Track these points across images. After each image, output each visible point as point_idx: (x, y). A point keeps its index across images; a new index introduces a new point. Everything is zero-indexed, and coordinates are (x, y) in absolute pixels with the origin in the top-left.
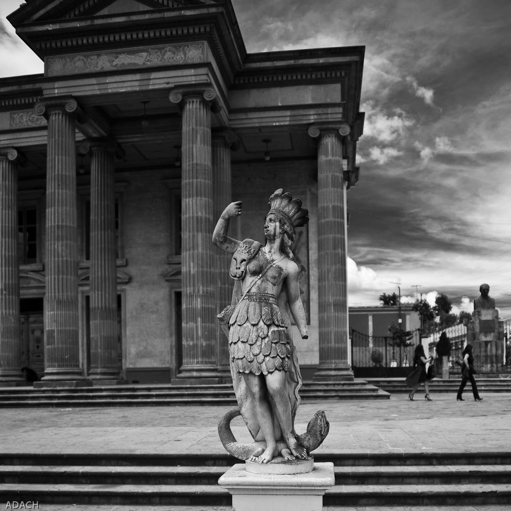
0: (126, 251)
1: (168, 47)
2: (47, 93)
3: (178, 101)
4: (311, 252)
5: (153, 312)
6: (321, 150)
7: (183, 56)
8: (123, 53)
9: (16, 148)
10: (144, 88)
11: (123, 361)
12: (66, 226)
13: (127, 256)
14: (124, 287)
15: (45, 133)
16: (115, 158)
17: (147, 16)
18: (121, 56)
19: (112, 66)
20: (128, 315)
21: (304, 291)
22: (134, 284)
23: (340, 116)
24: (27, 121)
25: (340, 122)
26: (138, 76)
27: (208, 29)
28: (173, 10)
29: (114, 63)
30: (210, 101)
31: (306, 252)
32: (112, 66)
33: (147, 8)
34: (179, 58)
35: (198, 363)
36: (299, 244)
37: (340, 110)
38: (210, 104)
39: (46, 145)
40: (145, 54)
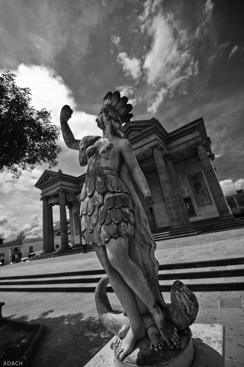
1: (146, 139)
4: (205, 182)
5: (162, 210)
8: (135, 144)
10: (142, 151)
11: (157, 226)
14: (152, 205)
17: (138, 133)
18: (135, 146)
20: (155, 212)
26: (140, 149)
27: (155, 130)
28: (144, 129)
31: (204, 182)
33: (137, 132)
34: (149, 140)
35: (176, 223)
37: (201, 137)
40: (140, 143)
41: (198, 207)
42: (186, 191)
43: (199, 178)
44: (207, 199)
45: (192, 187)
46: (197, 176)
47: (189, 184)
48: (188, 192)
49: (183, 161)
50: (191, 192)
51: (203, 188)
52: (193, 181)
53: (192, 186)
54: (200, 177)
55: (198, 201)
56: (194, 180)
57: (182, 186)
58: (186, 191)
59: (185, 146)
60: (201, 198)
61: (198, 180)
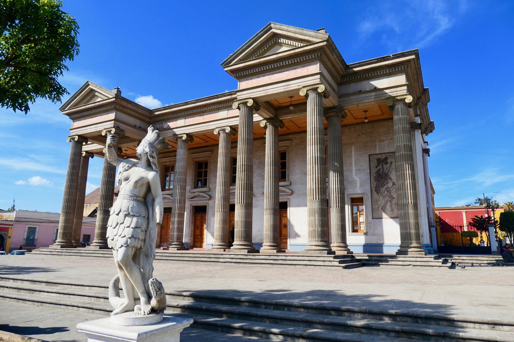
0: (290, 177)
2: (239, 98)
3: (304, 95)
6: (395, 112)
7: (307, 71)
9: (230, 126)
12: (249, 165)
13: (291, 180)
14: (289, 197)
15: (238, 118)
16: (279, 127)
19: (270, 80)
21: (396, 197)
22: (294, 195)
23: (406, 91)
24: (235, 113)
25: (406, 95)
27: (319, 55)
29: (272, 79)
30: (322, 92)
32: (270, 80)
36: (391, 169)
37: (406, 88)
38: (323, 94)
39: (238, 125)
41: (373, 218)
42: (358, 185)
43: (389, 164)
44: (393, 206)
45: (372, 178)
46: (386, 158)
47: (368, 171)
48: (362, 185)
49: (364, 123)
50: (368, 187)
51: (390, 185)
52: (377, 167)
53: (372, 177)
54: (391, 163)
55: (376, 206)
56: (378, 165)
57: (354, 172)
58: (358, 185)
59: (373, 97)
60: (382, 202)
61: (386, 167)
